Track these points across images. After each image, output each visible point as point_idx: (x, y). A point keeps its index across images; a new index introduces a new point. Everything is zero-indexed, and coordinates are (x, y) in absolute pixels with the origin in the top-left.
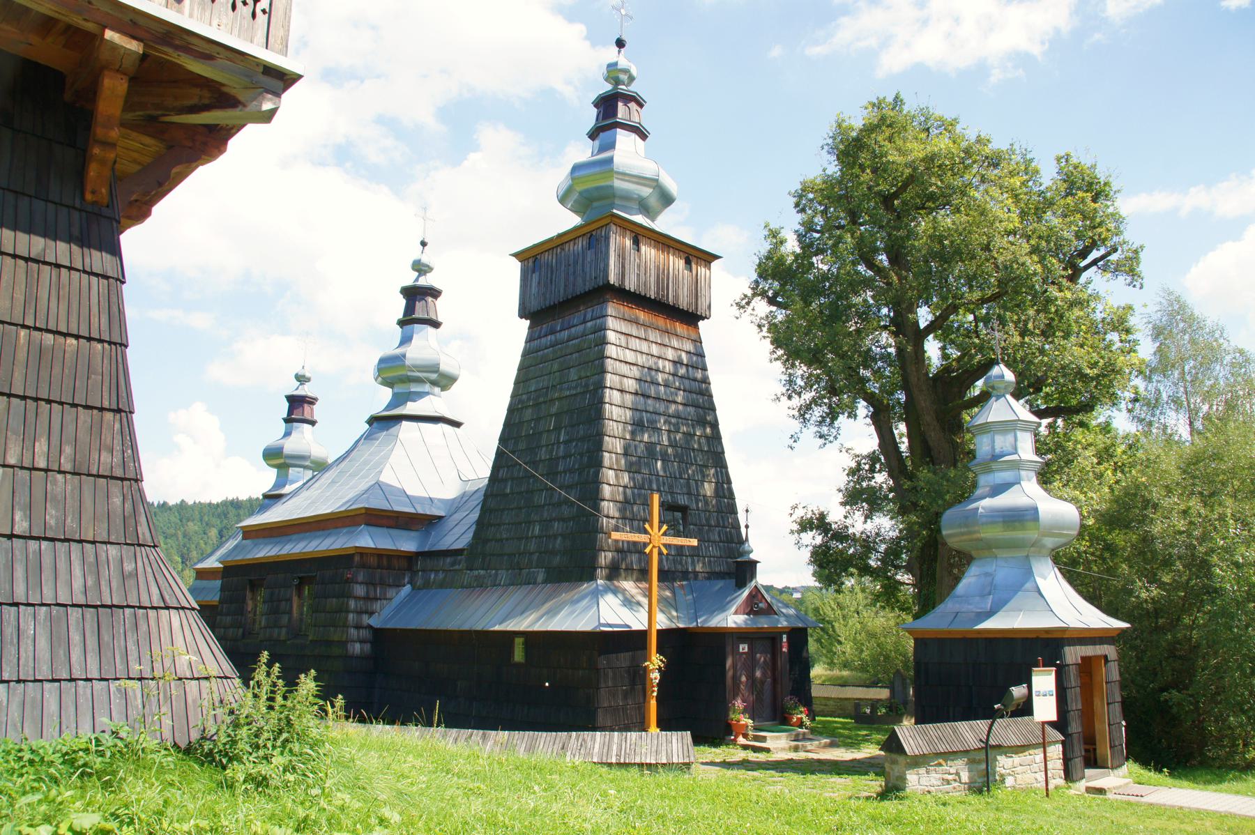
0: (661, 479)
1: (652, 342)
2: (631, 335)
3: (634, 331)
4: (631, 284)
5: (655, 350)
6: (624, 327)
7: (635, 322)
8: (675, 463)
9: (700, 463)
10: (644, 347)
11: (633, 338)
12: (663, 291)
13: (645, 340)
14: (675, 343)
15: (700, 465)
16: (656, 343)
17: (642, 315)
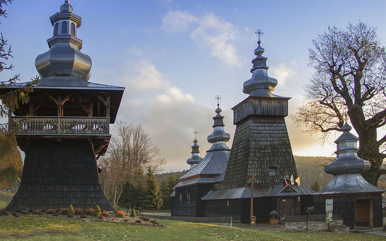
0: (268, 161)
1: (266, 127)
2: (259, 126)
3: (260, 125)
4: (259, 112)
5: (267, 128)
6: (256, 125)
7: (261, 123)
8: (273, 157)
9: (283, 155)
10: (263, 128)
11: (260, 127)
12: (269, 112)
13: (264, 126)
14: (275, 125)
15: (282, 156)
16: (268, 127)
17: (263, 120)
